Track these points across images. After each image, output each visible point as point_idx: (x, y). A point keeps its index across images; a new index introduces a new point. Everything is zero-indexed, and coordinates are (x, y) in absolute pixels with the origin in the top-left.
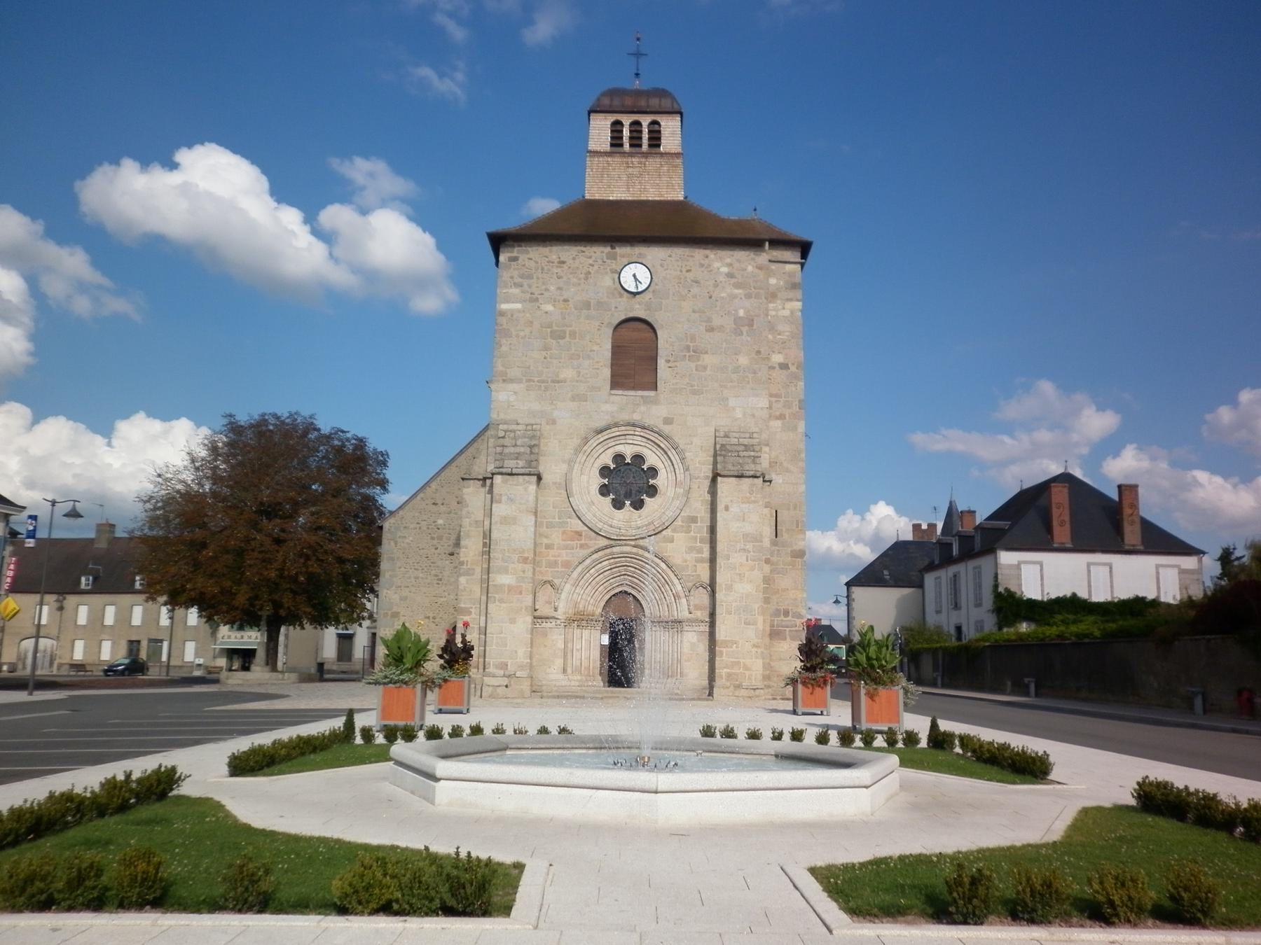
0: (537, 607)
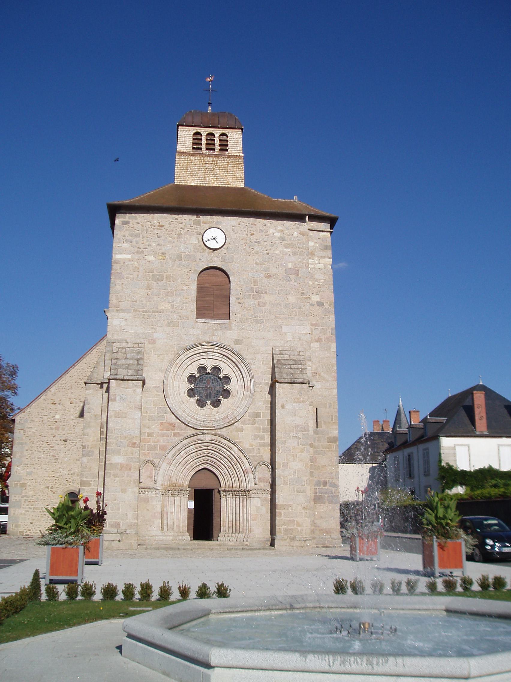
0: (141, 480)
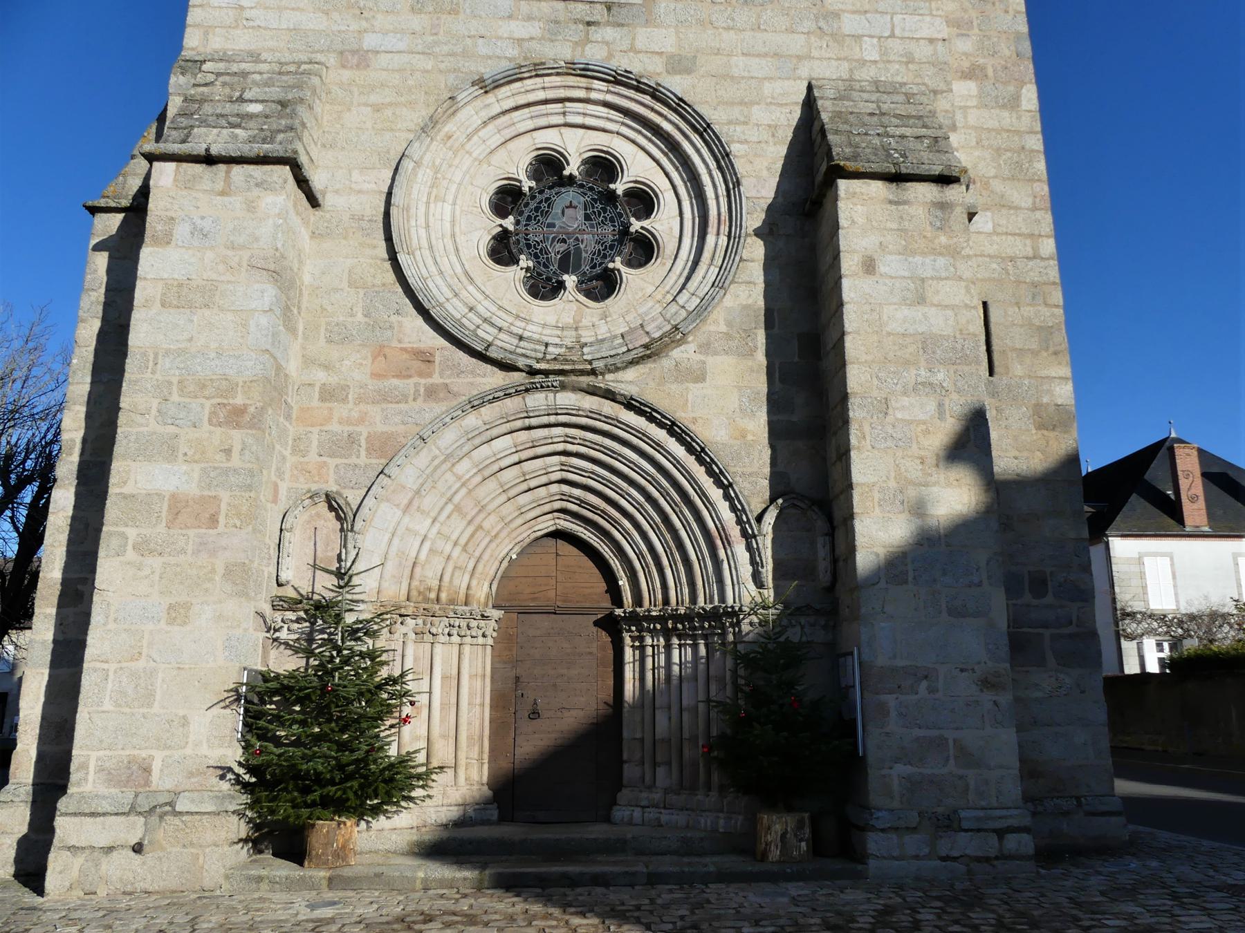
0: (284, 577)
